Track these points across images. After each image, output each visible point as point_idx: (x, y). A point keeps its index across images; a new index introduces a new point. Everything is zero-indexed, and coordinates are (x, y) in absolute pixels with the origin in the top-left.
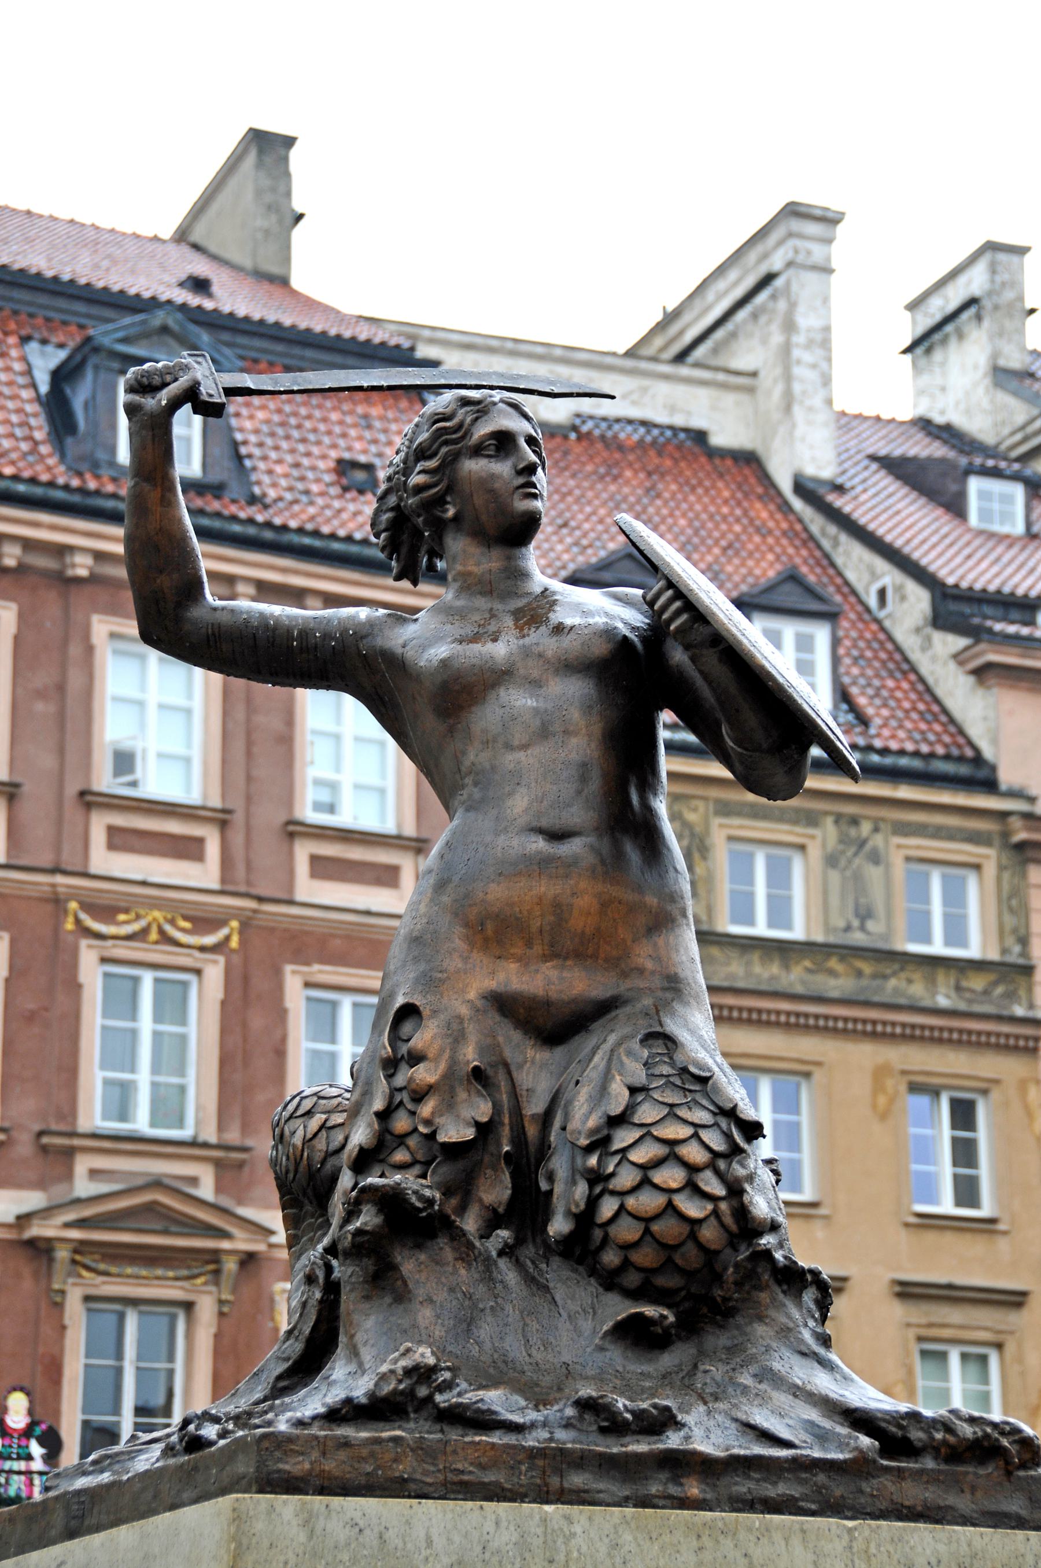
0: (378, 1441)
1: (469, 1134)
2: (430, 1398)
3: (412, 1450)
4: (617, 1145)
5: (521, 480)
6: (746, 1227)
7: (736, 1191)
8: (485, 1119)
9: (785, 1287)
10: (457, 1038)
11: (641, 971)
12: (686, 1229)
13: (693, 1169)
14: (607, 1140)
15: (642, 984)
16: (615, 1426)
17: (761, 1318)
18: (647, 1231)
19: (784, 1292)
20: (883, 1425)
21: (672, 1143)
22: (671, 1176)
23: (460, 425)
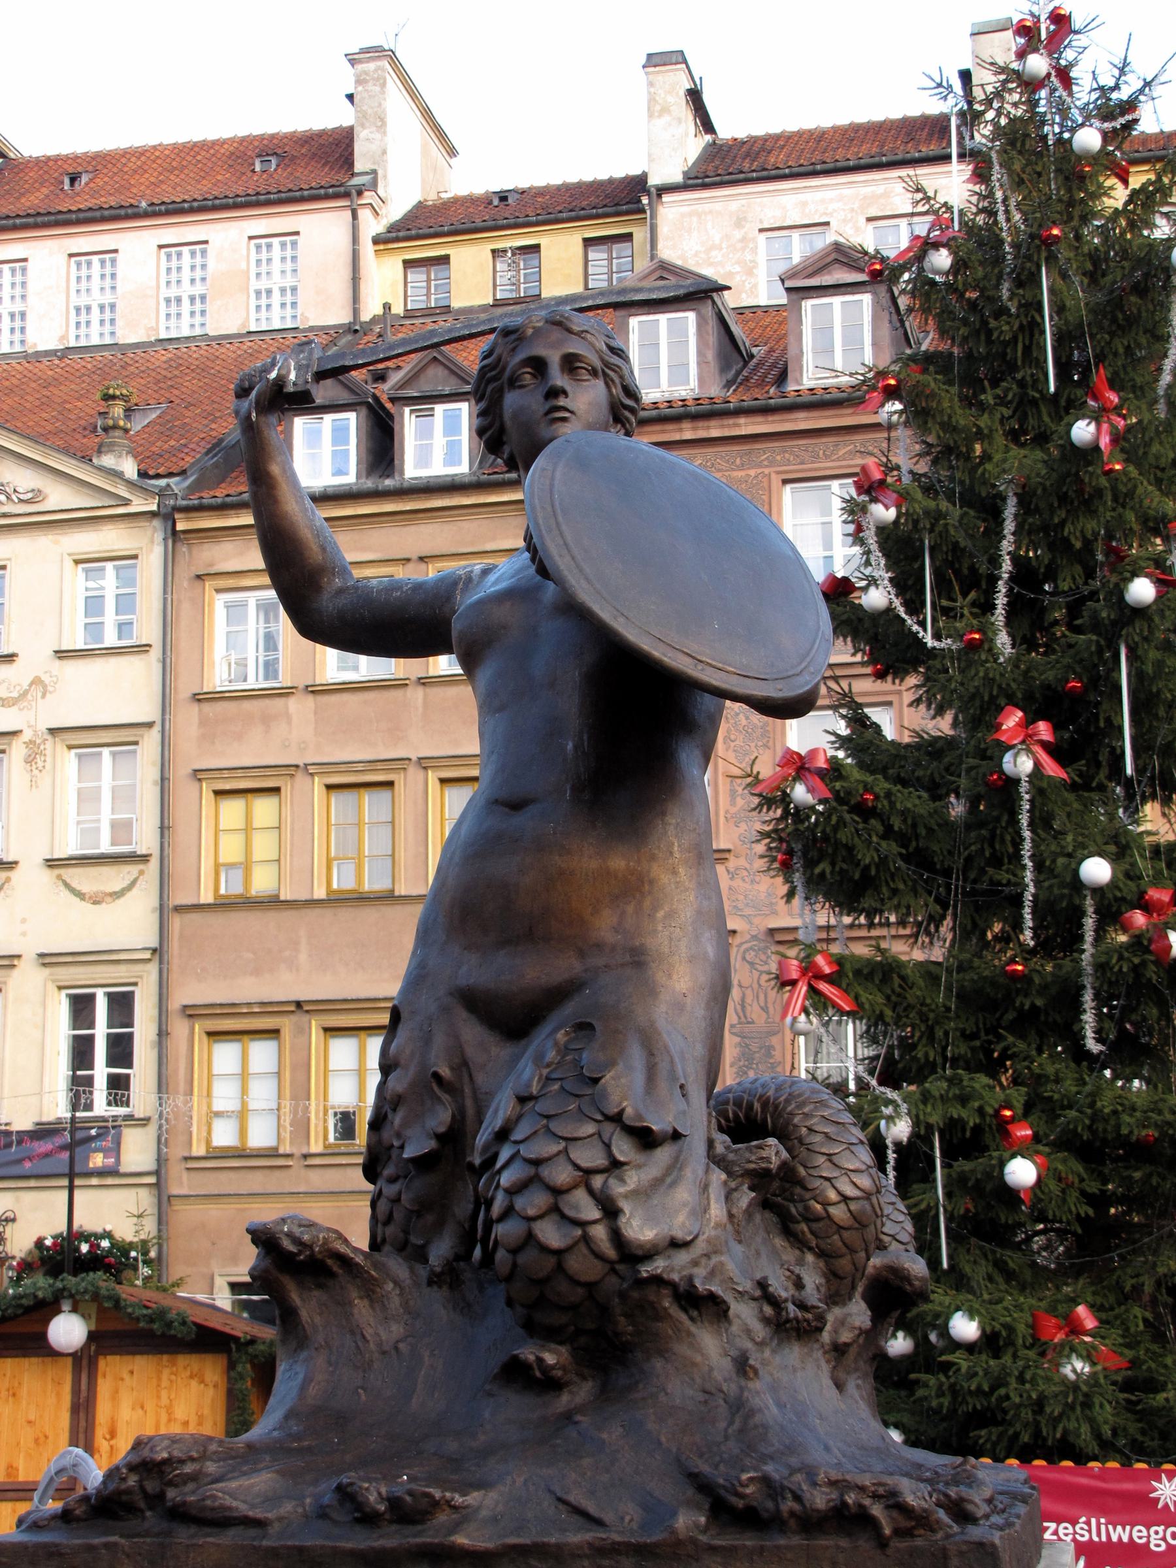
0: (91, 1548)
1: (430, 1145)
2: (161, 1496)
3: (128, 1556)
4: (499, 1165)
5: (547, 407)
6: (630, 1255)
7: (611, 1212)
8: (442, 1129)
9: (695, 1314)
10: (427, 1040)
11: (599, 946)
12: (552, 1260)
13: (557, 1192)
14: (495, 1156)
15: (600, 961)
16: (368, 1519)
17: (663, 1353)
18: (515, 1265)
19: (692, 1319)
20: (722, 1492)
21: (537, 1163)
22: (533, 1202)
23: (499, 359)
